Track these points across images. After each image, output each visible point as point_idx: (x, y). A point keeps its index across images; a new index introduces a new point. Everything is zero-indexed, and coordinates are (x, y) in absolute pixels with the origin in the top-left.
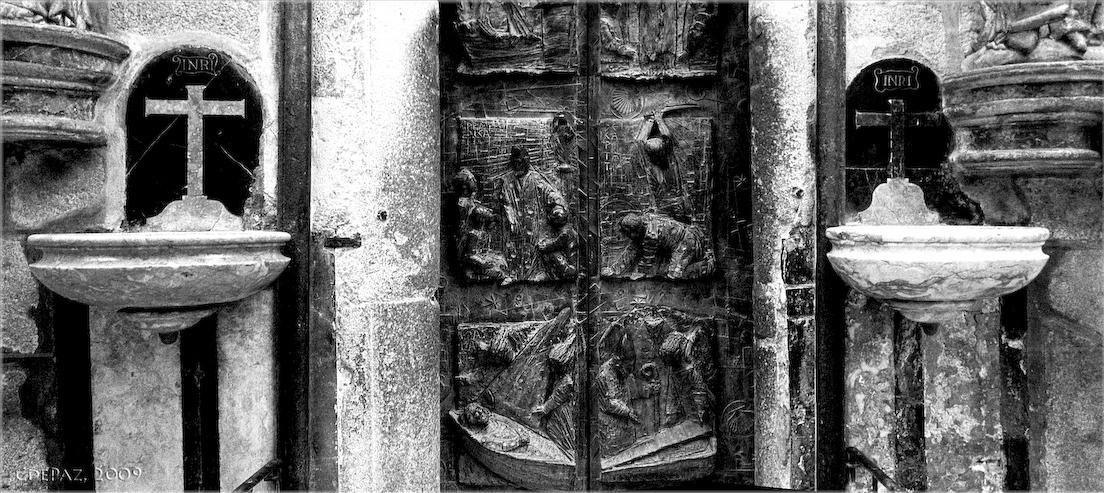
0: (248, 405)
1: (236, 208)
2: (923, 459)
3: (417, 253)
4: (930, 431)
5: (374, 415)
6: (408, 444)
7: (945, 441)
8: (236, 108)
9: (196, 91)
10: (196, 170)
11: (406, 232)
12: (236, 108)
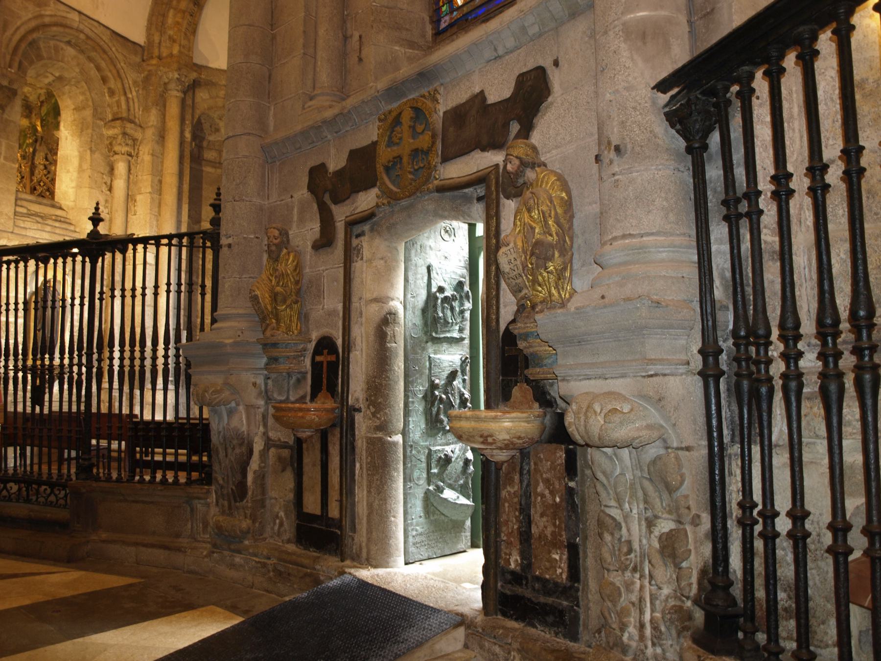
0: (335, 472)
1: (333, 397)
2: (530, 545)
3: (379, 416)
4: (534, 530)
5: (365, 483)
6: (375, 497)
7: (540, 536)
8: (332, 358)
9: (326, 351)
10: (325, 381)
11: (374, 407)
12: (332, 358)
